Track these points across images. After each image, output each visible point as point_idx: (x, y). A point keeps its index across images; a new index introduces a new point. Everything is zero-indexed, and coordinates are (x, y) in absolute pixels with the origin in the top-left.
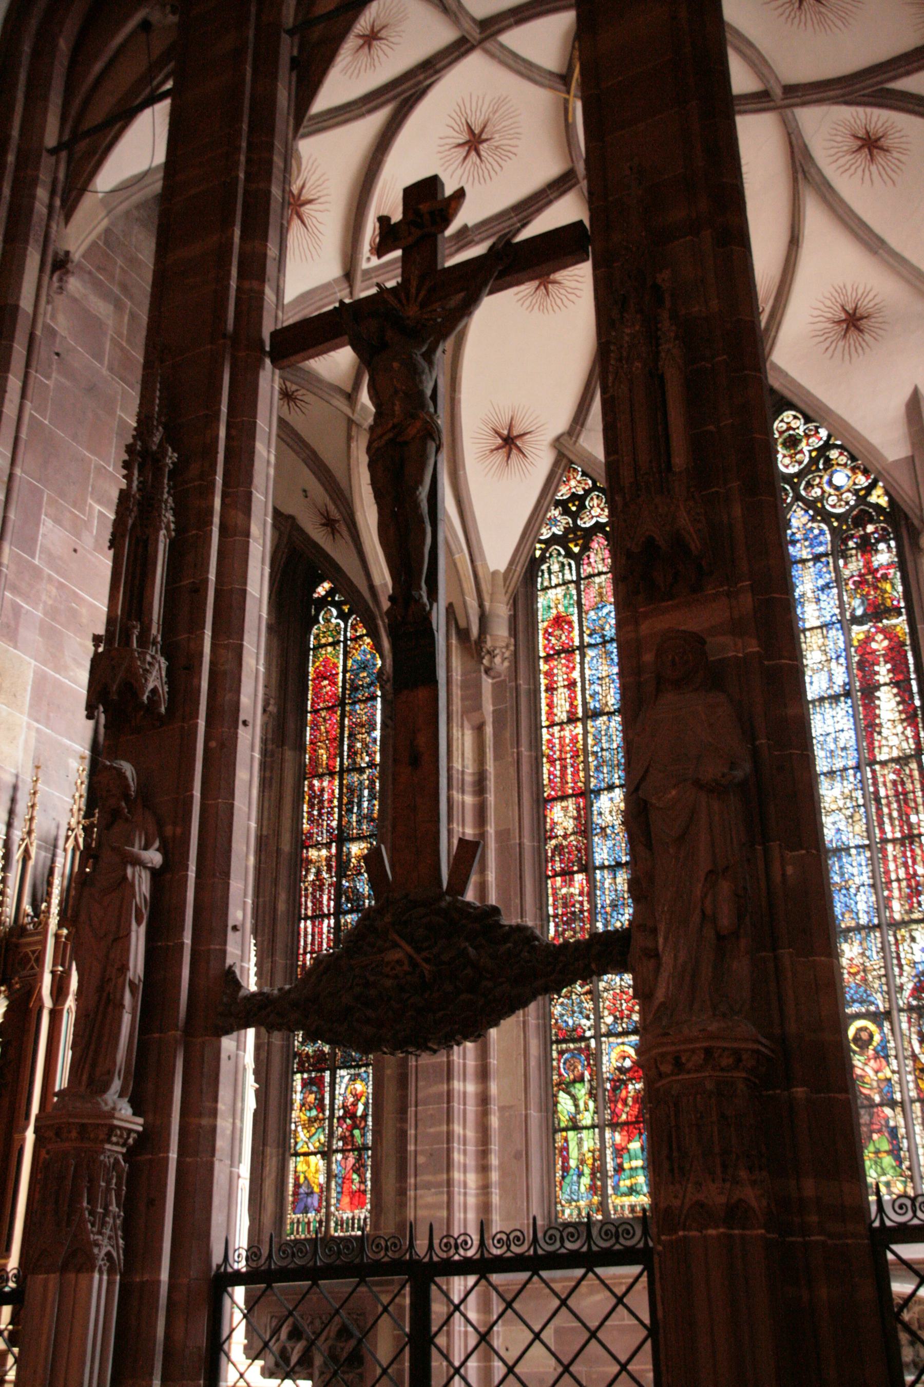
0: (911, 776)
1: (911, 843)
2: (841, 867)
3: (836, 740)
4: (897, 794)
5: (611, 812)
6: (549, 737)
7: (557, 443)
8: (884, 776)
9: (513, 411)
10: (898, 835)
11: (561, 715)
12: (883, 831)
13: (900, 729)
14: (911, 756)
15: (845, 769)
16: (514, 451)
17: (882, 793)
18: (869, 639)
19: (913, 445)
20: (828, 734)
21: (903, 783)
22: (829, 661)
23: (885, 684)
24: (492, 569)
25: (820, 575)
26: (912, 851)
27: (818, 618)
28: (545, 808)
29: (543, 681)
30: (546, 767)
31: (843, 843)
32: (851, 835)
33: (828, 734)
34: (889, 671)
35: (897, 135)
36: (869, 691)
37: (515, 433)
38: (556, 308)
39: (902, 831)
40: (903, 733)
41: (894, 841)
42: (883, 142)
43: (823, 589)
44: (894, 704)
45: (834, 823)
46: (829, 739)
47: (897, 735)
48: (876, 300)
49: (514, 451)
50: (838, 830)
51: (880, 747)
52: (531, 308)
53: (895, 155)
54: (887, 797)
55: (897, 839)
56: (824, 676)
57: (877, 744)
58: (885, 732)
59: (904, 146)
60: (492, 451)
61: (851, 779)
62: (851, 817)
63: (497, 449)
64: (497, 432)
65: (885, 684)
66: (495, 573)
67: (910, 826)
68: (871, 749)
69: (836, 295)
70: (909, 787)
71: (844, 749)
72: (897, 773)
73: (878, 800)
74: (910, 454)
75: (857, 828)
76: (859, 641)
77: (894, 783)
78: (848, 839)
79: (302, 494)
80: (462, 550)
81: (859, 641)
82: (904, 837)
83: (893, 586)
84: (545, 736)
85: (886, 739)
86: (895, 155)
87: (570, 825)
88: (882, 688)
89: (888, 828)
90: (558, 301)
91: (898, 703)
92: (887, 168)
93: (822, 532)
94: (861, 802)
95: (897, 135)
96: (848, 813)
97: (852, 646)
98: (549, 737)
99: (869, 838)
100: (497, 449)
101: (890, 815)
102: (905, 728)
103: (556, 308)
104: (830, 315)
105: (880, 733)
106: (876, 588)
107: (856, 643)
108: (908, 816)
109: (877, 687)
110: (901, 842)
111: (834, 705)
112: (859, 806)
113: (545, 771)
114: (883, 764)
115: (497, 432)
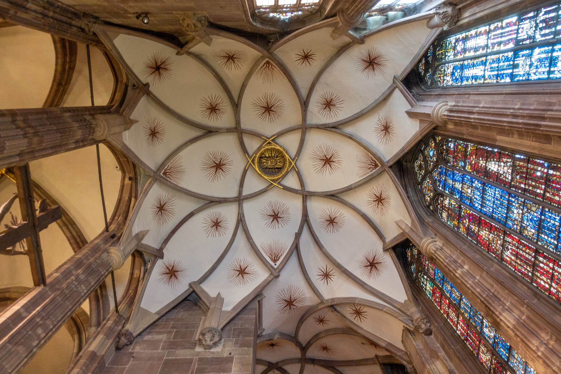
0: (521, 166)
1: (549, 181)
2: (548, 229)
3: (497, 199)
4: (526, 178)
5: (490, 331)
6: (460, 332)
7: (385, 250)
8: (517, 181)
9: (365, 257)
10: (543, 187)
11: (455, 320)
12: (538, 195)
13: (502, 164)
14: (513, 163)
15: (508, 201)
16: (376, 265)
17: (523, 186)
18: (470, 164)
19: (417, 118)
20: (494, 202)
21: (522, 173)
22: (472, 187)
23: (486, 164)
24: (403, 302)
25: (450, 175)
26: (553, 182)
27: (460, 183)
28: (480, 361)
29: (445, 316)
30: (467, 344)
31: (537, 221)
32: (535, 214)
33: (494, 202)
34: (482, 160)
35: (326, 95)
36: (487, 173)
37: (371, 261)
38: (343, 223)
39: (542, 184)
40: (504, 163)
41: (545, 191)
42: (329, 100)
43: (453, 177)
44: (493, 163)
45: (528, 221)
46: (496, 201)
47: (504, 166)
48: (383, 118)
49: (376, 265)
50: (531, 219)
51: (506, 178)
52: (338, 230)
53: (333, 97)
54: (525, 184)
55: (545, 188)
56: (476, 192)
57: (504, 179)
58: (501, 172)
59: (330, 94)
60: (370, 272)
61: (513, 200)
62: (528, 209)
63: (371, 270)
64: (366, 266)
65: (486, 164)
66: (405, 301)
67: (541, 177)
68: (505, 183)
69: (377, 131)
70: (525, 170)
71: (501, 198)
72: (518, 174)
73: (525, 190)
74: (419, 120)
75: (534, 209)
76: (470, 169)
77: (521, 177)
78: (536, 217)
79: (363, 345)
80: (385, 306)
81: (470, 169)
82: (545, 184)
83: (460, 145)
84: (459, 332)
85: (504, 172)
86: (333, 97)
87: (488, 357)
88: (487, 166)
89: (538, 191)
90: (341, 221)
91: (494, 161)
92: (338, 101)
93: (441, 168)
94: (523, 200)
95: (326, 95)
96: (525, 210)
97: (471, 173)
98: (460, 332)
99: (539, 205)
100: (371, 270)
101: (533, 186)
102: (503, 161)
103: (343, 223)
104: (383, 136)
105: (501, 175)
106: (458, 153)
107: (470, 171)
108: (537, 177)
109: (486, 167)
110: (547, 186)
111: (486, 193)
112: (524, 202)
113: (469, 346)
114: (512, 180)
115: (366, 266)
